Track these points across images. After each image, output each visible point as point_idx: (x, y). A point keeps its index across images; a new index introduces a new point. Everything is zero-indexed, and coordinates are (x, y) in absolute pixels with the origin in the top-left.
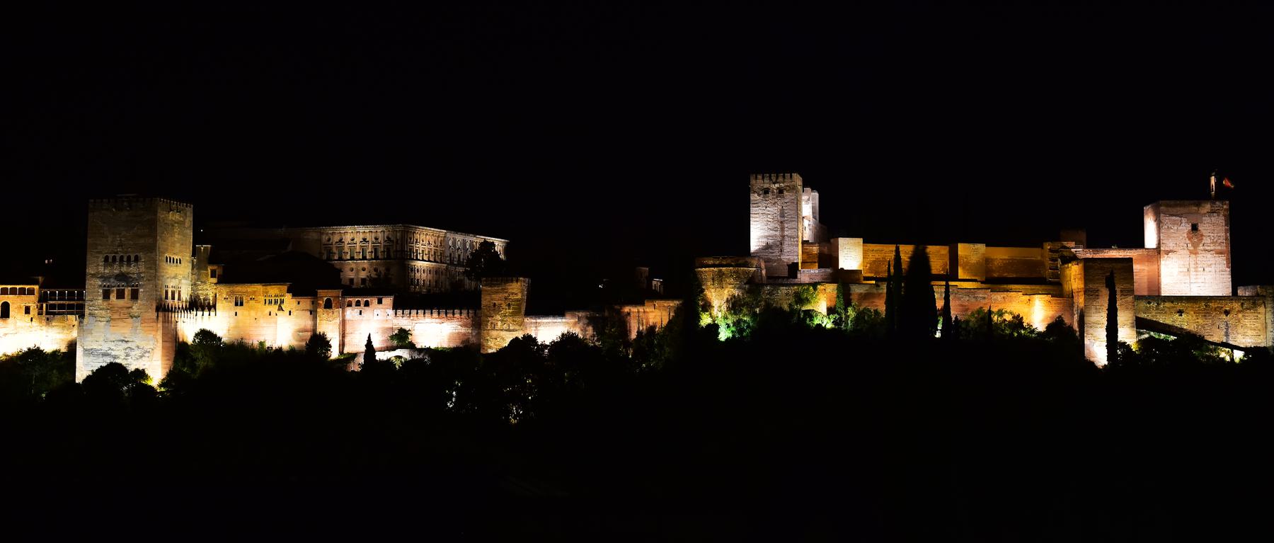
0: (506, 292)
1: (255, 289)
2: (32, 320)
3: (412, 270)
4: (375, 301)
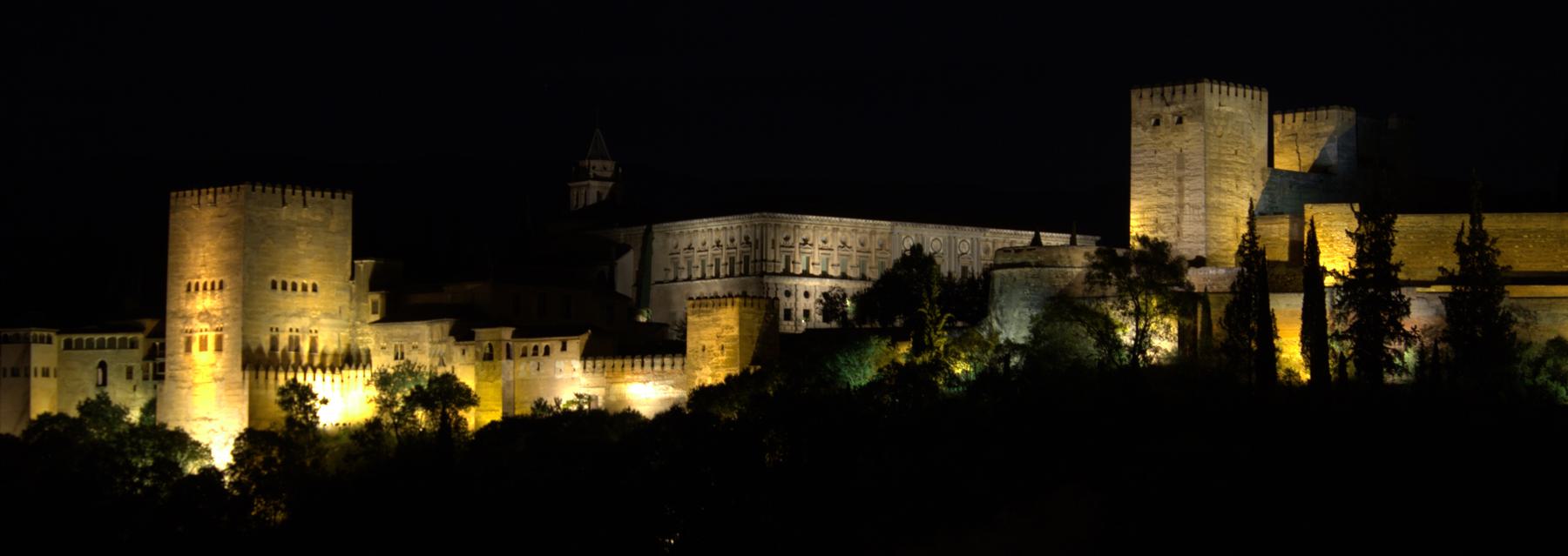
0: (719, 325)
1: (418, 332)
2: (135, 389)
3: (788, 294)
4: (555, 344)
